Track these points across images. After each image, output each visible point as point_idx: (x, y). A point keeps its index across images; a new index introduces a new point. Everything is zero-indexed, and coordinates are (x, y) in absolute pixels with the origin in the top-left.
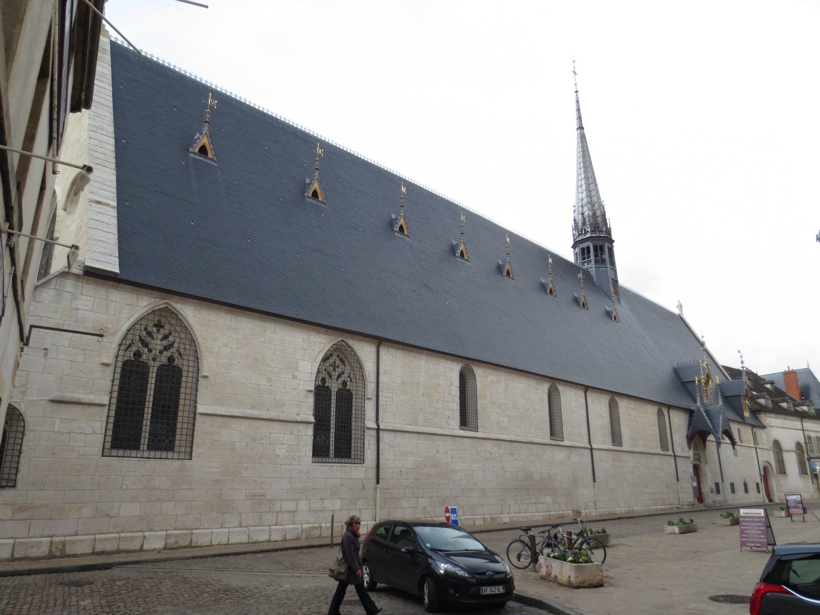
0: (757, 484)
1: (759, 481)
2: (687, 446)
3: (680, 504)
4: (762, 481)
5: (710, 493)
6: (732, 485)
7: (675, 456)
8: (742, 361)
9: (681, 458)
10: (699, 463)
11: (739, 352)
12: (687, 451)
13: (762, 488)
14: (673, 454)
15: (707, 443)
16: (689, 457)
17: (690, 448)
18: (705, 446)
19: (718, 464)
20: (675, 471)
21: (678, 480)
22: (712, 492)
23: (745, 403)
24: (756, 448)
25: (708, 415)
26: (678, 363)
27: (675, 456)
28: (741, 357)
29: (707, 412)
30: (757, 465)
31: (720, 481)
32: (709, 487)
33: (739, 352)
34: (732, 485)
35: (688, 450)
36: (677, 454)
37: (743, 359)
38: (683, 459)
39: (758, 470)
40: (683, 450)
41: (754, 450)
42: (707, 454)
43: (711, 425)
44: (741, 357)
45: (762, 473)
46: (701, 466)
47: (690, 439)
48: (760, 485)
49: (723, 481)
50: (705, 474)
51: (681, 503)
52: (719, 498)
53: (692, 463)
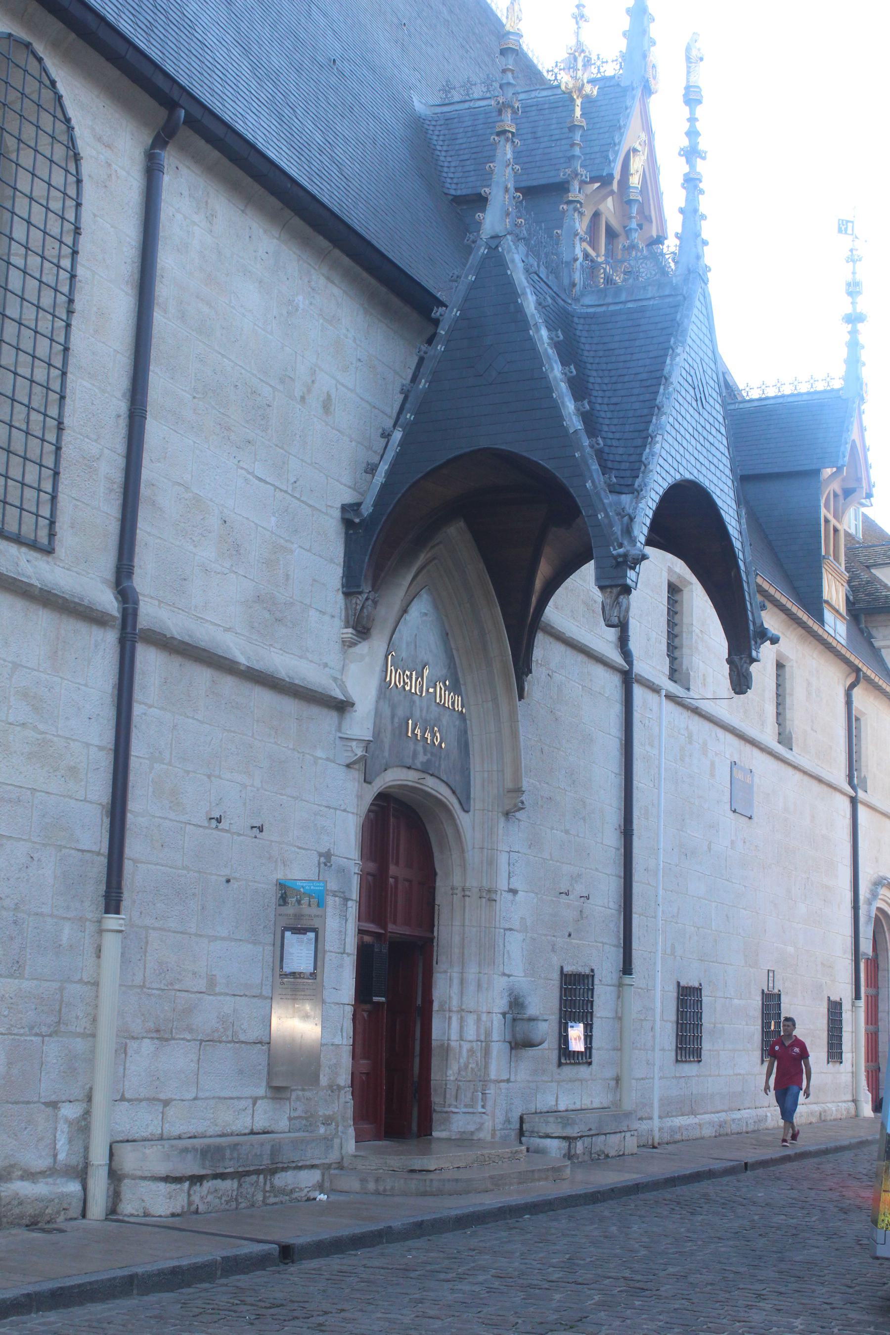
0: (835, 1009)
1: (843, 991)
2: (335, 601)
3: (82, 1173)
4: (857, 997)
5: (498, 1049)
6: (689, 999)
7: (130, 633)
8: (857, 284)
9: (228, 684)
10: (444, 793)
11: (843, 227)
12: (333, 656)
13: (855, 1032)
14: (107, 600)
15: (544, 650)
16: (342, 707)
17: (361, 628)
18: (522, 664)
19: (612, 839)
20: (99, 789)
21: (112, 901)
22: (520, 1043)
23: (836, 530)
24: (854, 801)
25: (569, 352)
26: (447, 89)
27: (130, 633)
28: (853, 259)
29: (561, 319)
30: (848, 896)
31: (603, 962)
32: (500, 1004)
33: (843, 227)
34: (689, 999)
35: (347, 645)
36: (151, 613)
37: (863, 305)
38: (263, 698)
39: (849, 930)
40: (271, 612)
41: (844, 805)
42: (525, 732)
43: (569, 406)
44: (853, 259)
45: (866, 947)
46: (464, 820)
47: (383, 543)
48: (847, 1016)
49: (627, 969)
50: (489, 895)
51: (99, 1156)
52: (576, 1095)
53: (366, 766)
